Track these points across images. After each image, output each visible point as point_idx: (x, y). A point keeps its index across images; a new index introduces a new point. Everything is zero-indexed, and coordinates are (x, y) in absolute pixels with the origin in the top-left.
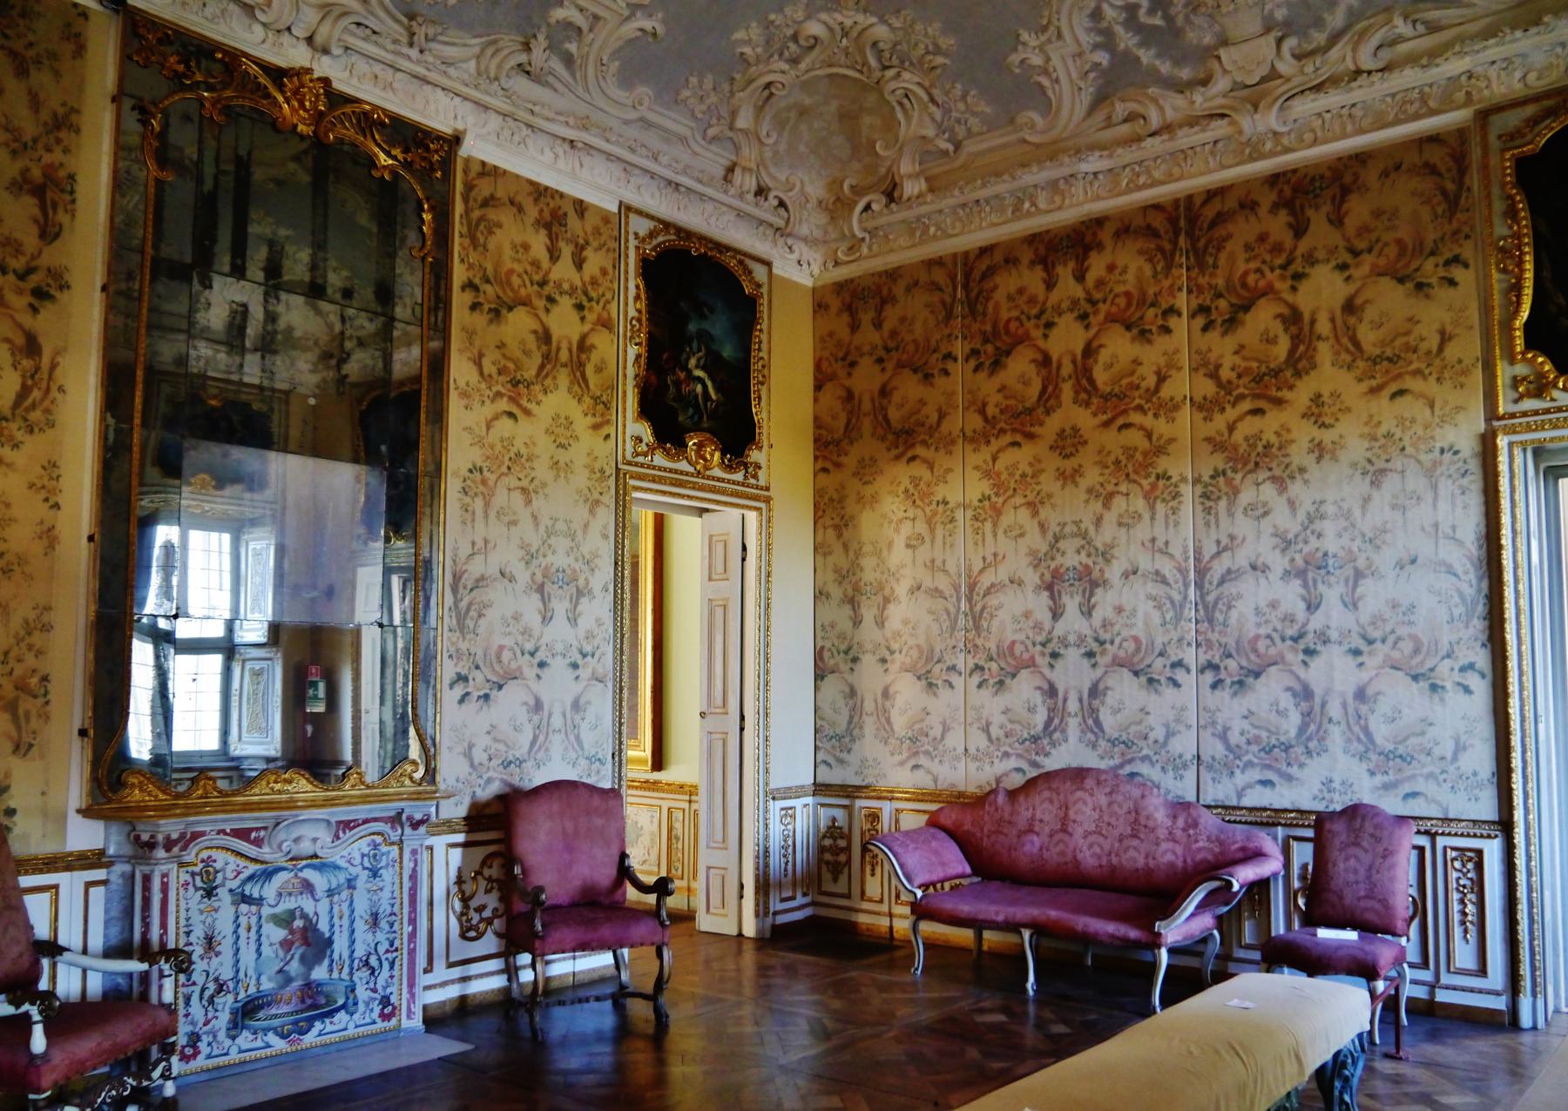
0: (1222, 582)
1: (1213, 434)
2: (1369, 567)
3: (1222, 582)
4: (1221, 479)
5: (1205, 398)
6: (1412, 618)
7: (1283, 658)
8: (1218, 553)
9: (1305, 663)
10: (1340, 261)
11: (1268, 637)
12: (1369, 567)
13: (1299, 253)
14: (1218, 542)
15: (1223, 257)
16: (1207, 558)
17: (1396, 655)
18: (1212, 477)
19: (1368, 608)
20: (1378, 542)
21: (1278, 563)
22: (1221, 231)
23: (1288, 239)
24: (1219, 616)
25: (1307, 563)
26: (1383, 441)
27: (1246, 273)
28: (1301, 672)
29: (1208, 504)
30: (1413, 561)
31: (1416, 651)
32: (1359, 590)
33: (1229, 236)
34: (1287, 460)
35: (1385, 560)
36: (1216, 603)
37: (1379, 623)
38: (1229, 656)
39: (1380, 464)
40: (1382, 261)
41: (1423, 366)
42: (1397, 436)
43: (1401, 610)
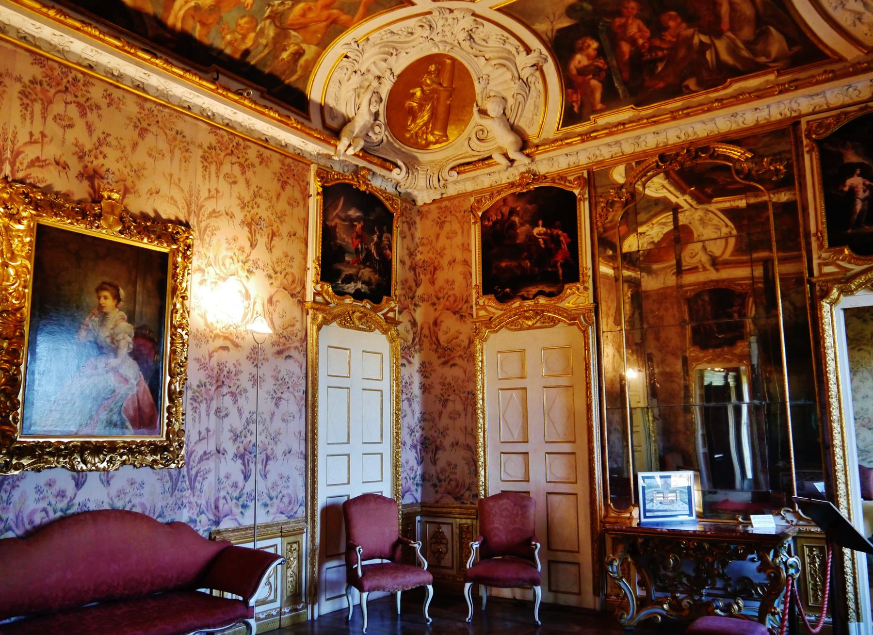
0: (201, 460)
1: (201, 357)
2: (272, 454)
3: (201, 460)
4: (203, 389)
5: (197, 330)
6: (289, 484)
7: (231, 511)
8: (200, 440)
9: (242, 513)
10: (268, 272)
11: (225, 498)
12: (272, 454)
13: (251, 258)
14: (200, 433)
15: (214, 240)
16: (193, 444)
17: (282, 505)
18: (198, 386)
19: (272, 477)
20: (277, 440)
21: (231, 449)
22: (213, 222)
23: (247, 248)
24: (198, 485)
25: (245, 450)
26: (281, 381)
27: (224, 258)
28: (239, 517)
29: (195, 405)
30: (290, 452)
31: (290, 503)
32: (268, 467)
33: (218, 229)
34: (238, 383)
35: (279, 449)
36: (196, 476)
37: (275, 487)
38: (202, 513)
39: (279, 394)
40: (285, 282)
41: (299, 346)
42: (286, 380)
43: (284, 479)
